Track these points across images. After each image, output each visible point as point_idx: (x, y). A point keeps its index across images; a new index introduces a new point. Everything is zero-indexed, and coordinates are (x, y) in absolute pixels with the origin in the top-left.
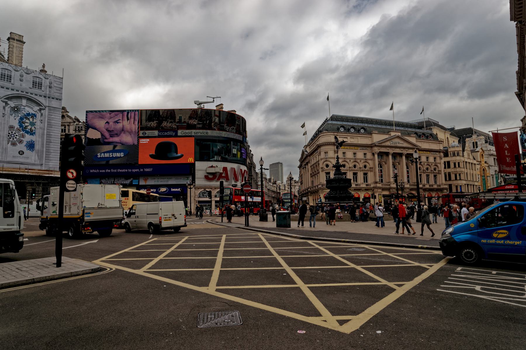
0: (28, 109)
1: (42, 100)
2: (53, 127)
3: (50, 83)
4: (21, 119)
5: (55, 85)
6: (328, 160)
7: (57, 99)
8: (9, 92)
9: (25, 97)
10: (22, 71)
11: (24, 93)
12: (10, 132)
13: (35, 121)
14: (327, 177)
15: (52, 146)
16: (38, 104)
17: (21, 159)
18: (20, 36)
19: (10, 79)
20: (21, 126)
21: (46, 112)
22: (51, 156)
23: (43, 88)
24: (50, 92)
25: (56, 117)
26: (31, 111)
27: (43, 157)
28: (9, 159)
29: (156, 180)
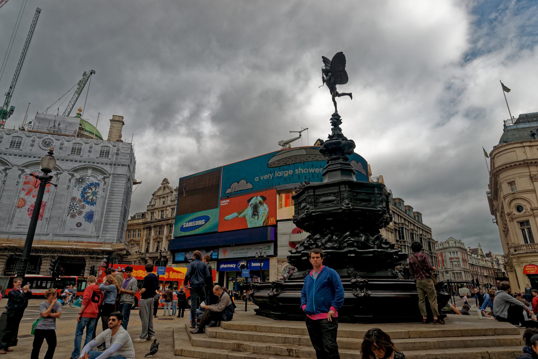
0: (91, 177)
1: (107, 168)
2: (115, 194)
3: (118, 150)
4: (85, 189)
5: (123, 151)
6: (518, 196)
7: (123, 165)
8: (77, 165)
9: (90, 168)
10: (92, 143)
11: (91, 164)
12: (72, 204)
13: (97, 190)
14: (523, 230)
15: (111, 216)
16: (102, 172)
17: (78, 232)
18: (120, 116)
19: (80, 152)
20: (83, 197)
21: (109, 181)
22: (109, 227)
23: (110, 156)
24: (116, 159)
25: (120, 184)
26: (95, 181)
27: (100, 228)
28: (66, 232)
29: (235, 252)
